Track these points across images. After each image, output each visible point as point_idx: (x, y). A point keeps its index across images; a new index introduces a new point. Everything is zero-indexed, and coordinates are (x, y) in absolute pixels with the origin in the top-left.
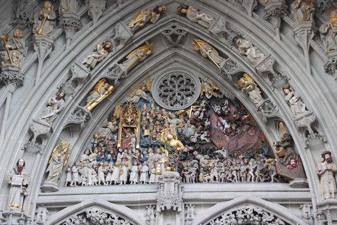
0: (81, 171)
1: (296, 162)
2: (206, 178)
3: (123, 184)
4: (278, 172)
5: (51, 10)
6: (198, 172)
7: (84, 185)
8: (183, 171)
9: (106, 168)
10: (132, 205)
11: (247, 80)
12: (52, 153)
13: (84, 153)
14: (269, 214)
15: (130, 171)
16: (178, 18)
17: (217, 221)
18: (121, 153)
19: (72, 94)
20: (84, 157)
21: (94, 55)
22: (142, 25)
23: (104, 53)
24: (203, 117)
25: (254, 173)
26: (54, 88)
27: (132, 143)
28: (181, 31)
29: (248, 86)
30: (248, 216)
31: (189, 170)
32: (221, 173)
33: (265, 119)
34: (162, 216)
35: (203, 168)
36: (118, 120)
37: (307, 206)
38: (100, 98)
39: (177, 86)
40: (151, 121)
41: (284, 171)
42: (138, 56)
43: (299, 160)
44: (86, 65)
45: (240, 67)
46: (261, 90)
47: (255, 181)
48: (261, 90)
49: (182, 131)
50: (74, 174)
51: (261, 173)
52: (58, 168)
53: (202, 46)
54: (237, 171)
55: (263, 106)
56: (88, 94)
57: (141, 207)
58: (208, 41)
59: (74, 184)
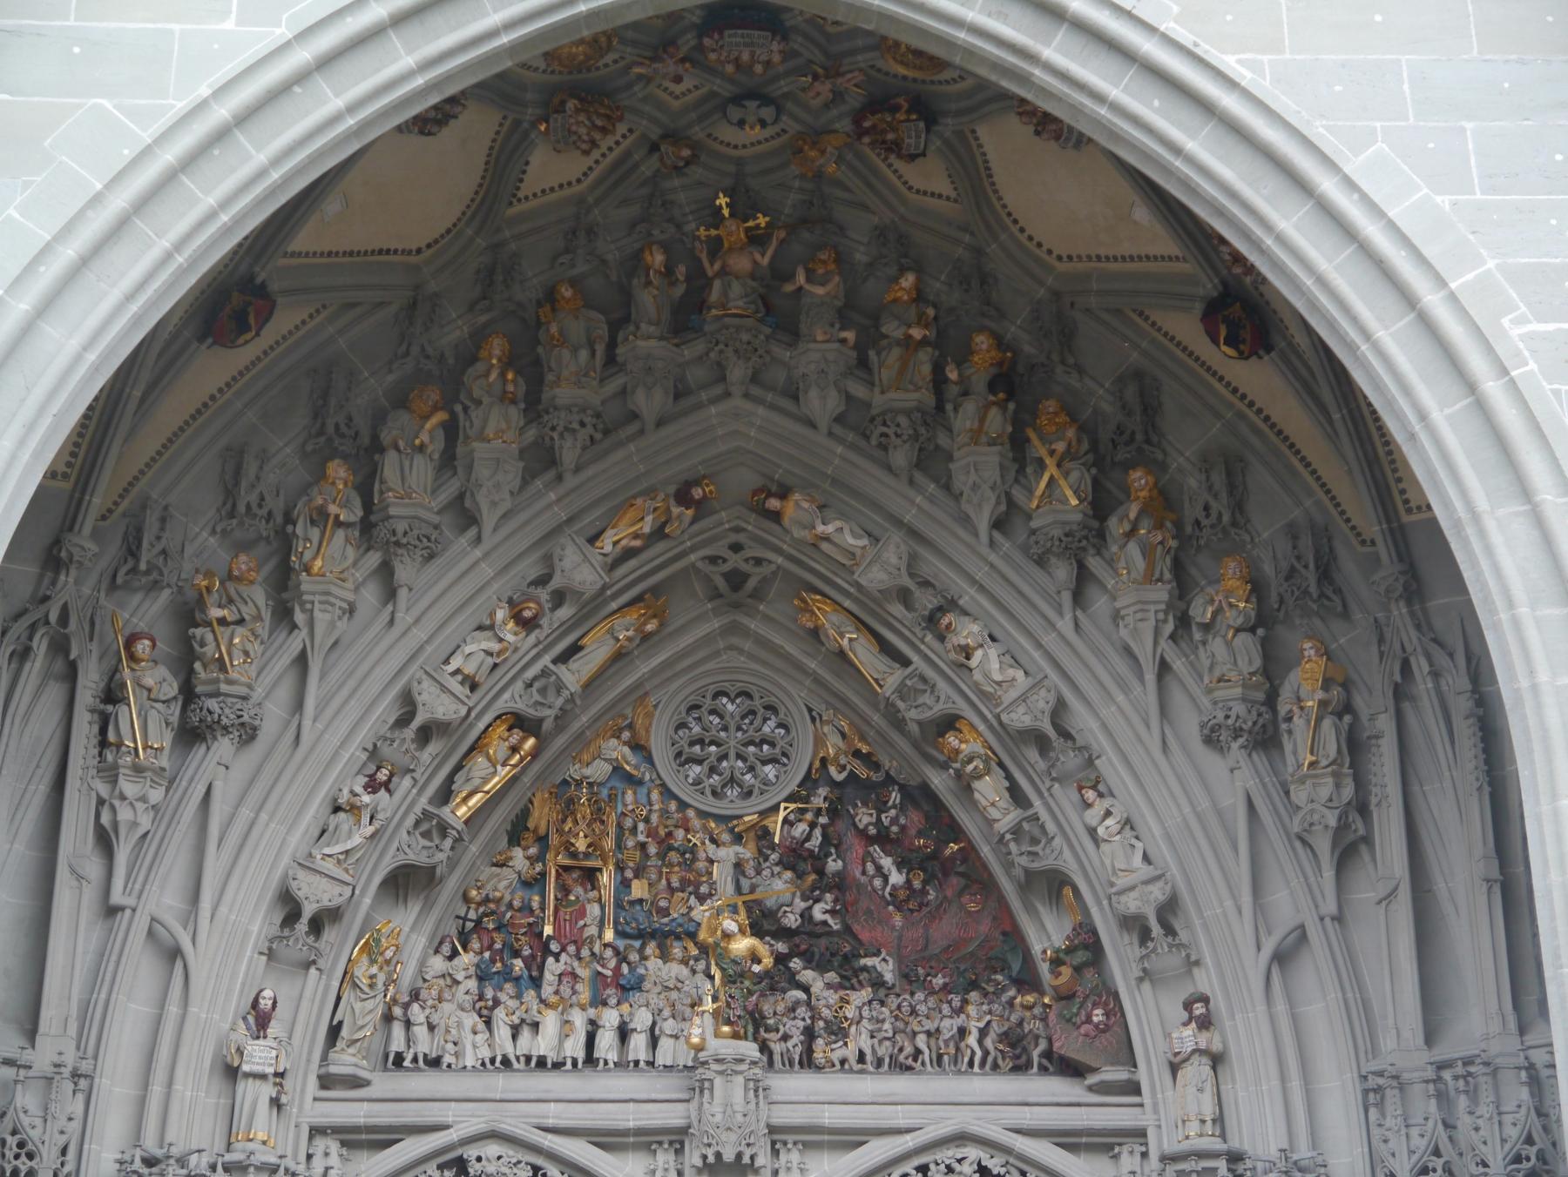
0: (435, 1019)
1: (1107, 1014)
2: (836, 1057)
3: (575, 1064)
4: (1056, 1045)
5: (346, 484)
6: (810, 1034)
7: (449, 1066)
8: (762, 1030)
9: (517, 1013)
11: (965, 744)
12: (350, 960)
16: (752, 524)
19: (413, 771)
20: (438, 964)
21: (485, 645)
22: (637, 543)
23: (516, 634)
25: (980, 1042)
26: (352, 750)
29: (970, 760)
31: (781, 1027)
32: (880, 1042)
33: (1018, 872)
35: (826, 1022)
37: (1131, 1152)
38: (496, 779)
41: (1070, 1045)
42: (618, 640)
43: (1115, 1010)
44: (459, 677)
45: (945, 699)
46: (1009, 776)
47: (983, 1064)
48: (1009, 776)
50: (415, 1029)
51: (1000, 1042)
52: (371, 1011)
53: (828, 619)
54: (929, 1034)
55: (1016, 831)
56: (458, 768)
58: (847, 603)
59: (415, 1060)
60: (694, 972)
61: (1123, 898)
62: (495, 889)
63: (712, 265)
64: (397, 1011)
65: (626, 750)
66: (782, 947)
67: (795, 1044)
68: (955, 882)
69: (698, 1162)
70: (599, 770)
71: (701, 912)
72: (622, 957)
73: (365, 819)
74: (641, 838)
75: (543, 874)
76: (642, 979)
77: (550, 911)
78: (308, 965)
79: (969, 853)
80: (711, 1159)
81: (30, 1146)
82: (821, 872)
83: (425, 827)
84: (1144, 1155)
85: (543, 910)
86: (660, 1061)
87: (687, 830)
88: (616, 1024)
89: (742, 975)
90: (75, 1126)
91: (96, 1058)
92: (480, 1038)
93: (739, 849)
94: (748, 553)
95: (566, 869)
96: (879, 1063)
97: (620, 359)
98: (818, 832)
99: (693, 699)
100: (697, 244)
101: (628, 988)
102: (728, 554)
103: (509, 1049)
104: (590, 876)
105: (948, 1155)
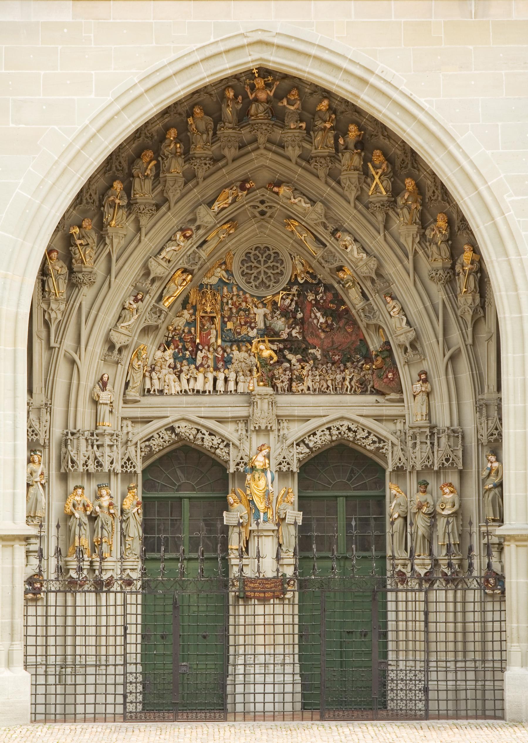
1: (394, 375)
2: (300, 389)
6: (291, 380)
10: (221, 420)
13: (158, 349)
14: (363, 430)
15: (215, 380)
17: (311, 438)
18: (201, 351)
20: (159, 354)
24: (295, 309)
25: (350, 383)
27: (212, 336)
28: (271, 207)
30: (342, 433)
34: (255, 433)
35: (296, 376)
36: (195, 308)
39: (262, 263)
40: (234, 311)
49: (271, 324)
54: (332, 380)
57: (231, 422)
59: (154, 391)
60: (250, 356)
61: (399, 337)
62: (178, 326)
63: (252, 94)
64: (147, 374)
65: (224, 273)
66: (281, 346)
67: (286, 384)
68: (343, 321)
69: (253, 429)
70: (214, 280)
71: (253, 333)
72: (224, 351)
73: (135, 312)
74: (230, 306)
75: (195, 320)
76: (232, 358)
77: (198, 334)
78: (117, 363)
79: (347, 311)
80: (257, 428)
81: (36, 432)
82: (295, 318)
83: (154, 310)
84: (405, 423)
85: (195, 332)
86: (239, 391)
87: (246, 302)
88: (223, 378)
89: (266, 364)
90: (48, 423)
91: (51, 399)
92: (177, 384)
93: (265, 309)
94: (265, 205)
95: (203, 317)
96: (315, 390)
97: (218, 136)
98: (294, 303)
99: (247, 251)
100: (246, 86)
101: (227, 362)
102: (259, 204)
103: (187, 388)
104: (212, 319)
105: (337, 424)
